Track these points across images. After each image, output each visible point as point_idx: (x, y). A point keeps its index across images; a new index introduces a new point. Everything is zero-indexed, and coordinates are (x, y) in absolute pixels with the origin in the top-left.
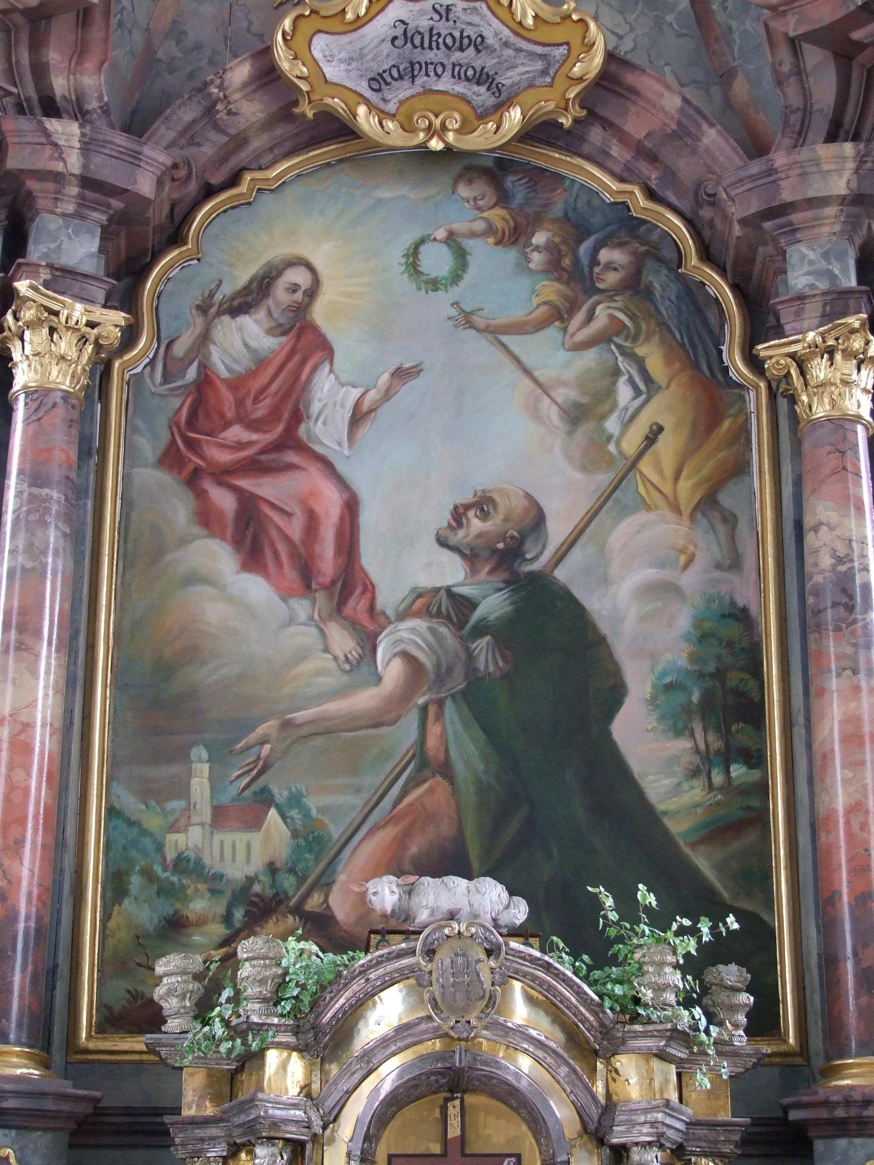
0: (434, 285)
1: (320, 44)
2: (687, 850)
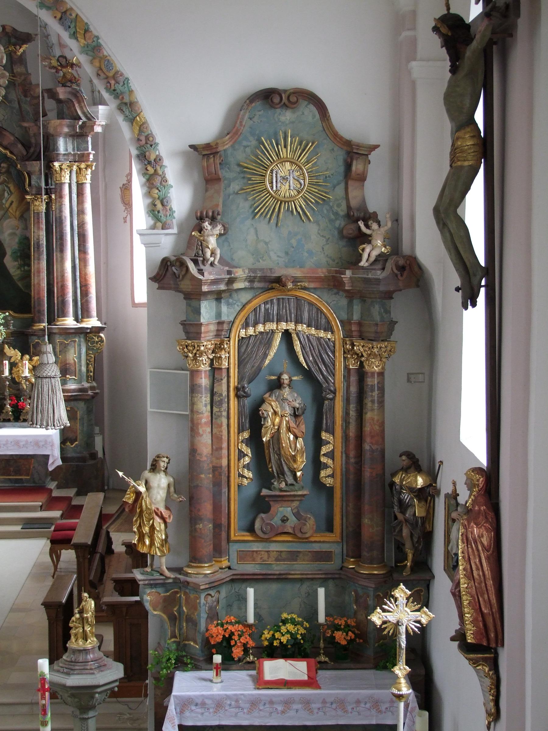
2: (17, 282)
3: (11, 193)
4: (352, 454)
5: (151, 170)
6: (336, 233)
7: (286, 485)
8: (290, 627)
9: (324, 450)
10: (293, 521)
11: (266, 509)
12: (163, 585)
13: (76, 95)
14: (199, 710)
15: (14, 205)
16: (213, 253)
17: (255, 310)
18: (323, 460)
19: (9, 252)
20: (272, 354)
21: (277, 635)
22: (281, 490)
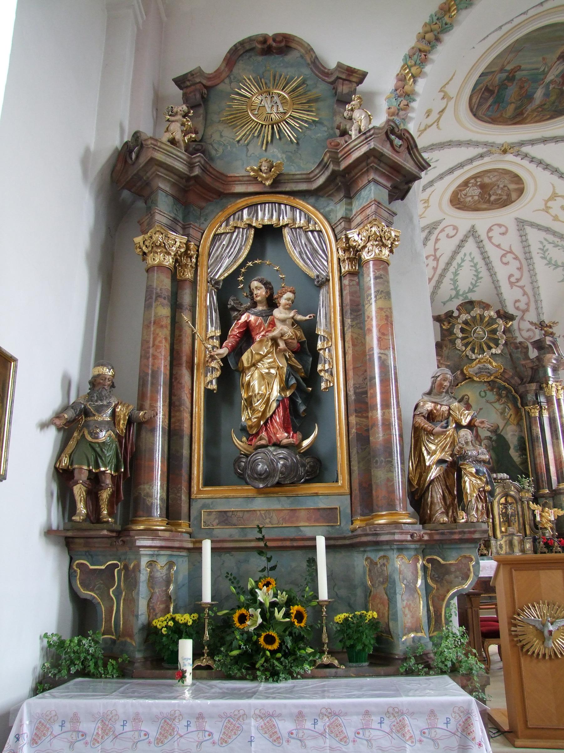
0: (483, 397)
1: (469, 369)
3: (510, 409)
15: (513, 417)
19: (512, 447)
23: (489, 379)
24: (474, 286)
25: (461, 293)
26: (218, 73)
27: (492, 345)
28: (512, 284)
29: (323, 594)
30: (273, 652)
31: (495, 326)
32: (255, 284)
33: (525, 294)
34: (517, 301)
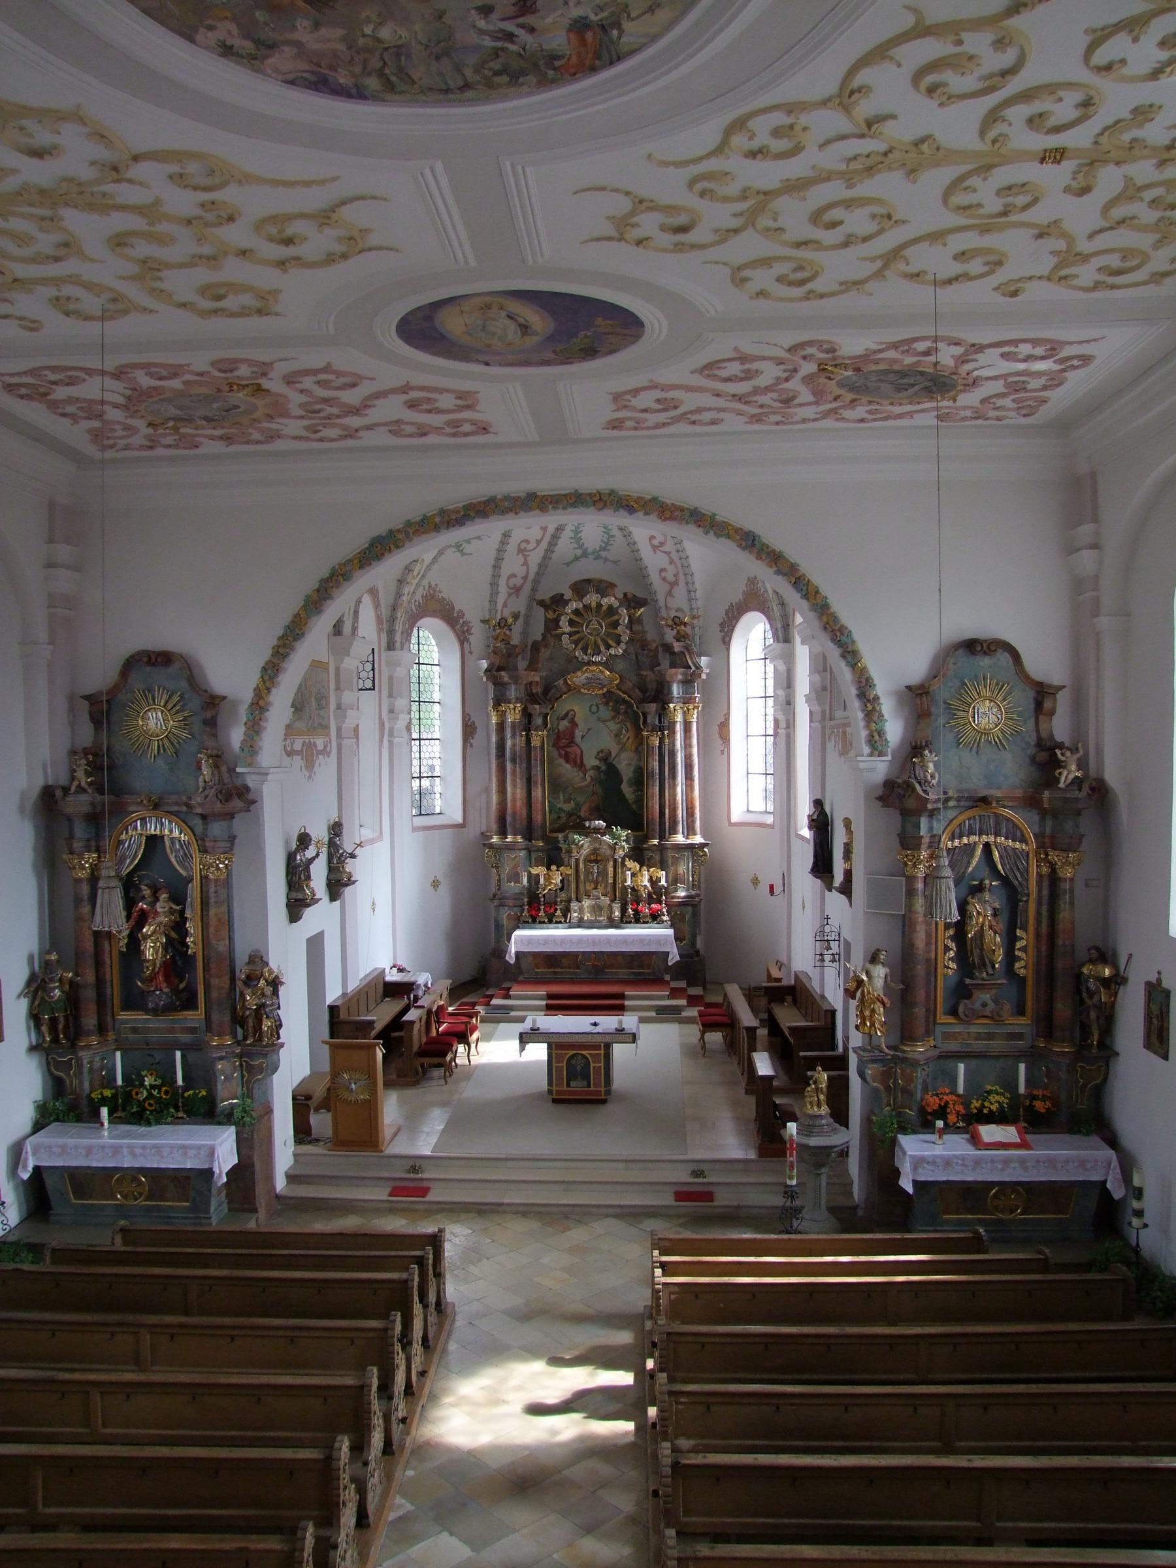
0: (594, 713)
3: (627, 731)
4: (1044, 948)
5: (870, 707)
6: (1027, 760)
7: (987, 974)
8: (997, 1098)
9: (1018, 945)
10: (991, 1005)
11: (969, 996)
12: (881, 1061)
13: (687, 648)
14: (930, 1168)
15: (630, 740)
16: (933, 776)
17: (960, 824)
18: (1017, 953)
19: (625, 779)
20: (975, 862)
21: (986, 1104)
22: (983, 979)
23: (601, 692)
24: (607, 544)
25: (590, 550)
26: (113, 691)
27: (611, 642)
28: (655, 548)
29: (180, 1082)
30: (151, 1111)
31: (615, 618)
32: (144, 887)
33: (672, 562)
34: (662, 570)
